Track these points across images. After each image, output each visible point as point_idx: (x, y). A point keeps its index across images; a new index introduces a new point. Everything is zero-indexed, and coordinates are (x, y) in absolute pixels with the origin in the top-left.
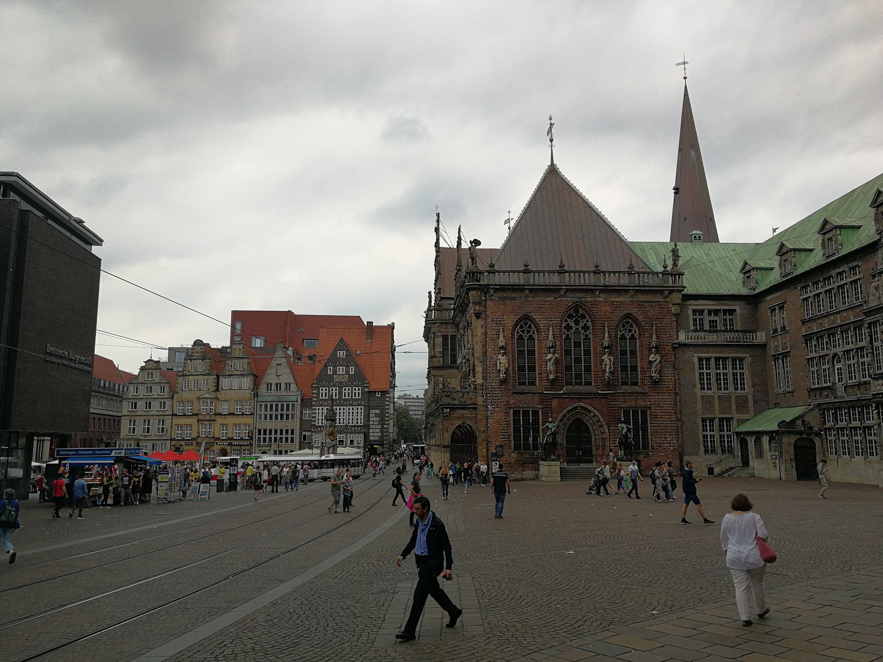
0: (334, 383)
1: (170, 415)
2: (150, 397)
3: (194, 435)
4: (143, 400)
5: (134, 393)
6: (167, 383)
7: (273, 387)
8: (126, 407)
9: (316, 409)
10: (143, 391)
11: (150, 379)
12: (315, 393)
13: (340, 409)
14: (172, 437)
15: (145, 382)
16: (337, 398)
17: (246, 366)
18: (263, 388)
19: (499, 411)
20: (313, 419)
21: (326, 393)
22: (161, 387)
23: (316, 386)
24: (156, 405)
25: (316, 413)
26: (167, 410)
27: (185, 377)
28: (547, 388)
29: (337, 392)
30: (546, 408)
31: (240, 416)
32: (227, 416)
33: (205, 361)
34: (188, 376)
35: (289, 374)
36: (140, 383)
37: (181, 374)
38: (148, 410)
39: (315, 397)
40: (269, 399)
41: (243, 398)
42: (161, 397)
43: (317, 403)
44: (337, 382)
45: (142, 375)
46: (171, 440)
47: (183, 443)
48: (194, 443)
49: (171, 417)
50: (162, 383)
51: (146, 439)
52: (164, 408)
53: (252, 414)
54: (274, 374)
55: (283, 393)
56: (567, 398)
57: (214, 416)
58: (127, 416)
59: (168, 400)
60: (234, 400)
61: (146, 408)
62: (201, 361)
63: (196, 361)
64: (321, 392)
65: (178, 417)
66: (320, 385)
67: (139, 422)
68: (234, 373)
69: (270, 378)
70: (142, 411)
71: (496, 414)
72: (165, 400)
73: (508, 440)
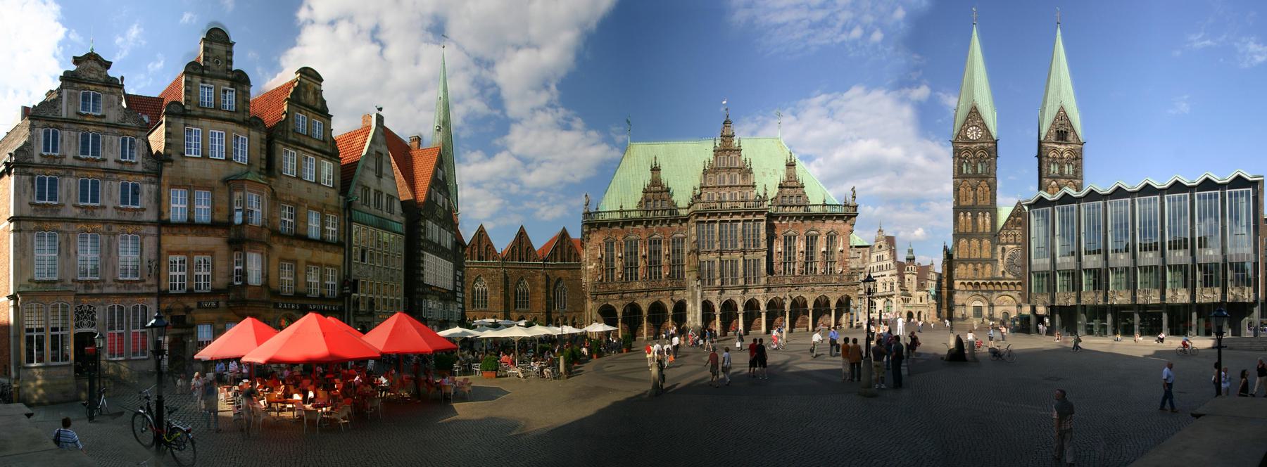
2: (95, 165)
3: (221, 282)
5: (47, 149)
8: (25, 192)
10: (73, 144)
14: (163, 287)
15: (78, 118)
22: (124, 141)
26: (143, 210)
27: (189, 121)
33: (239, 88)
34: (197, 117)
36: (65, 121)
38: (89, 203)
42: (126, 167)
45: (69, 98)
46: (162, 295)
47: (193, 304)
48: (222, 304)
49: (153, 230)
50: (129, 128)
51: (89, 292)
52: (135, 202)
62: (228, 84)
65: (175, 230)
70: (76, 206)
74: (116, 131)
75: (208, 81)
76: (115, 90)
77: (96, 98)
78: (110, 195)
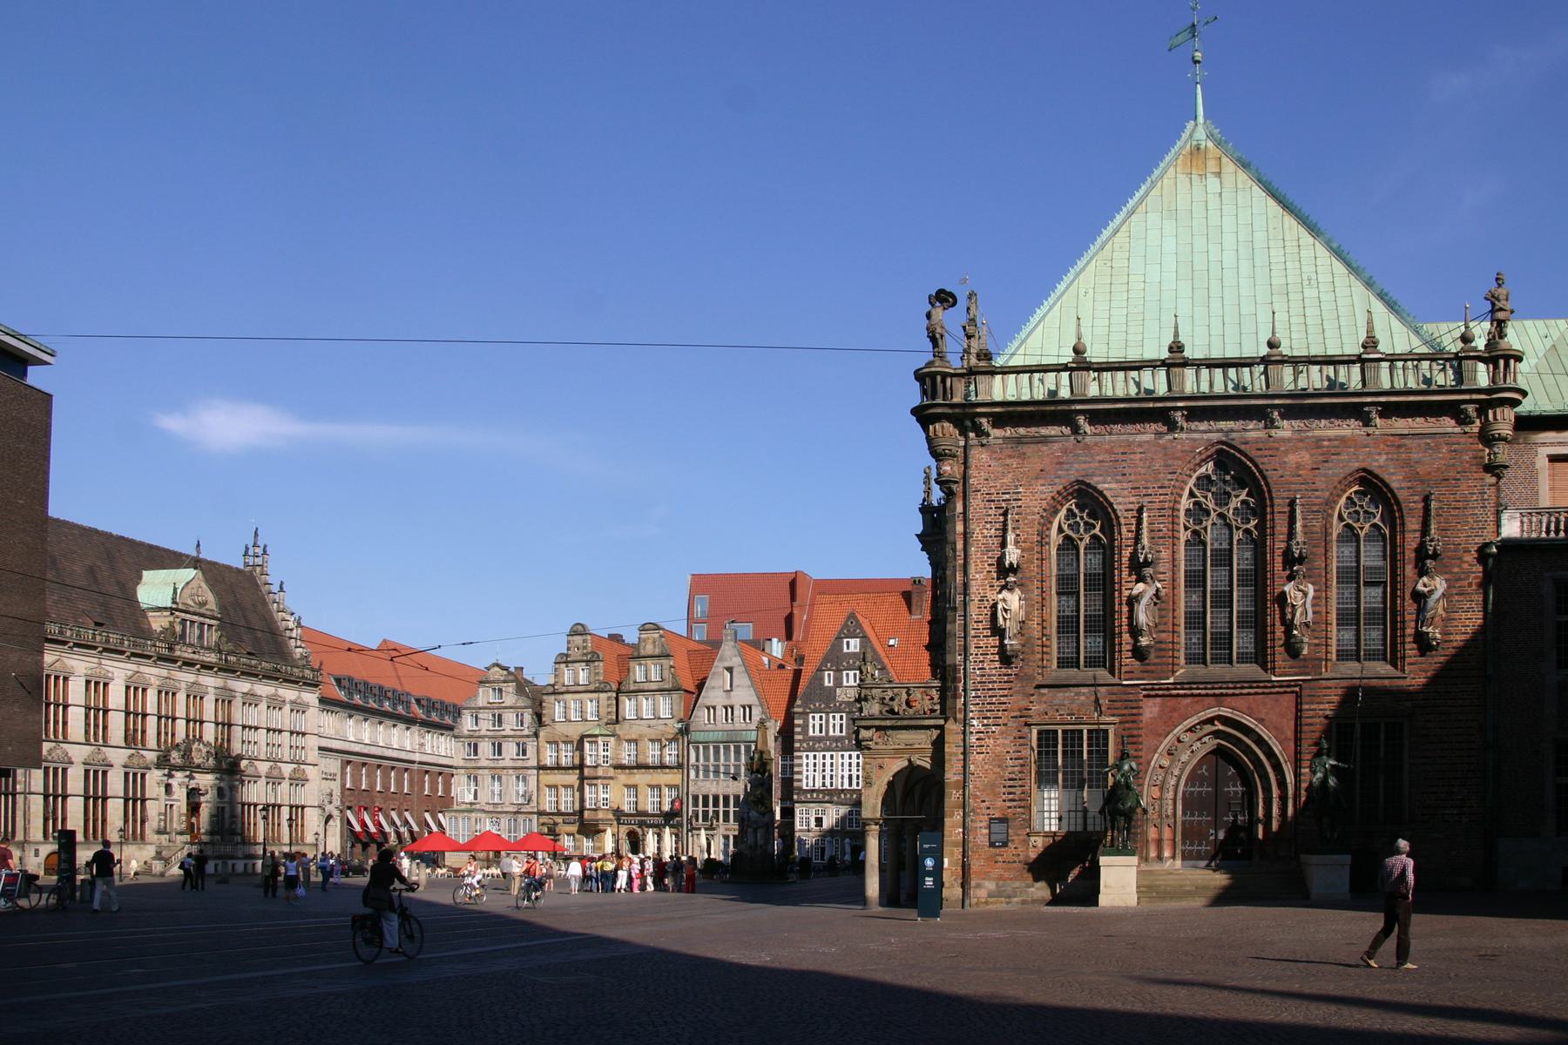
0: (838, 704)
1: (533, 768)
4: (487, 739)
6: (526, 707)
7: (721, 712)
9: (801, 757)
11: (497, 701)
12: (799, 726)
13: (850, 757)
15: (489, 705)
16: (844, 734)
17: (666, 673)
18: (701, 716)
19: (1002, 733)
20: (796, 777)
21: (821, 725)
22: (517, 715)
23: (800, 710)
24: (510, 749)
25: (801, 765)
26: (528, 759)
28: (1132, 672)
29: (844, 722)
30: (1127, 722)
31: (659, 770)
32: (635, 771)
33: (591, 664)
34: (562, 693)
35: (749, 687)
37: (551, 690)
38: (496, 757)
39: (799, 733)
40: (712, 737)
41: (663, 735)
42: (518, 733)
43: (805, 745)
44: (843, 702)
45: (483, 692)
49: (535, 772)
50: (519, 708)
51: (496, 810)
53: (680, 766)
54: (719, 687)
55: (737, 726)
56: (1185, 696)
57: (612, 770)
58: (462, 768)
59: (530, 739)
60: (646, 739)
61: (494, 755)
62: (584, 664)
63: (575, 665)
64: (811, 720)
66: (810, 709)
67: (483, 779)
68: (646, 686)
69: (714, 695)
71: (992, 741)
72: (525, 740)
73: (1022, 804)
74: (511, 710)
75: (570, 665)
76: (510, 684)
77: (500, 690)
78: (508, 752)
